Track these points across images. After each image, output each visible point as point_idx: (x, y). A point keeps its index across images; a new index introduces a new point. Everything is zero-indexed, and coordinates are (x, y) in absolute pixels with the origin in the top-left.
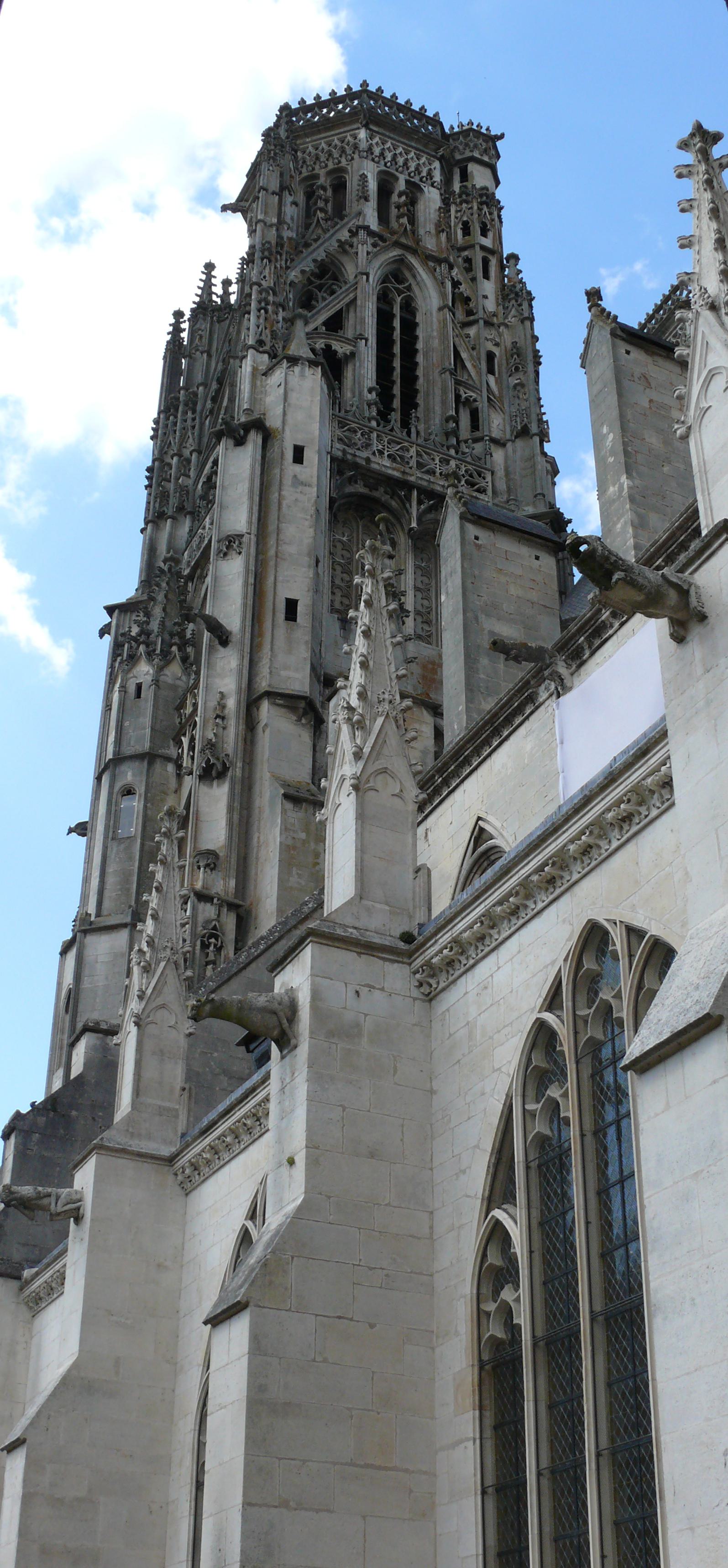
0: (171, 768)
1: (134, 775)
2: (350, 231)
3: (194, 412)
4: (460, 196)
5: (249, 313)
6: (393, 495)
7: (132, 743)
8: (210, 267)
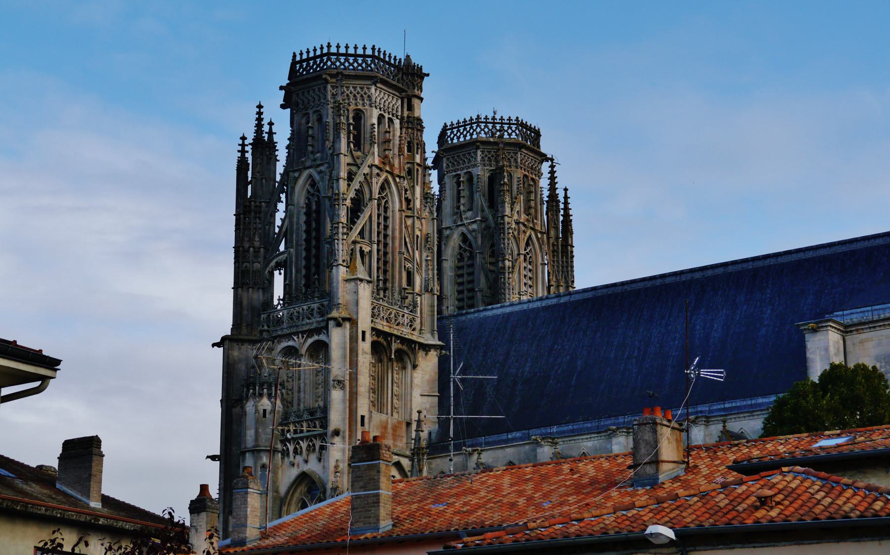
0: (280, 455)
1: (266, 459)
2: (369, 166)
3: (260, 218)
4: (408, 122)
5: (338, 240)
6: (386, 339)
7: (264, 441)
8: (260, 107)
